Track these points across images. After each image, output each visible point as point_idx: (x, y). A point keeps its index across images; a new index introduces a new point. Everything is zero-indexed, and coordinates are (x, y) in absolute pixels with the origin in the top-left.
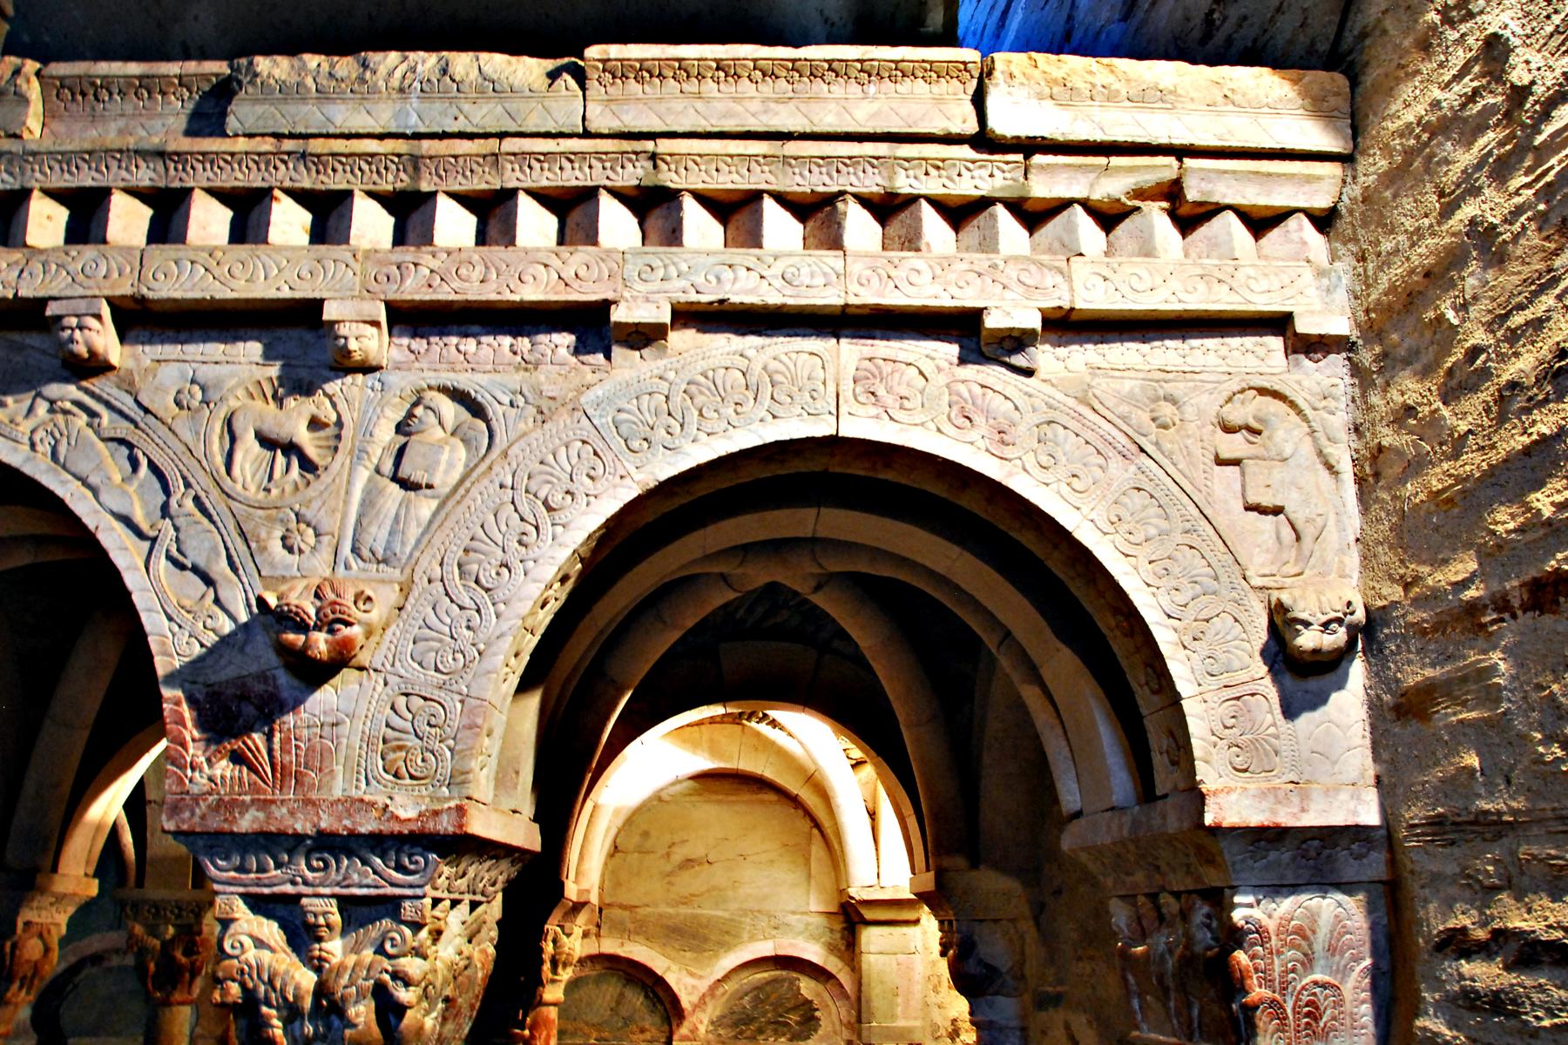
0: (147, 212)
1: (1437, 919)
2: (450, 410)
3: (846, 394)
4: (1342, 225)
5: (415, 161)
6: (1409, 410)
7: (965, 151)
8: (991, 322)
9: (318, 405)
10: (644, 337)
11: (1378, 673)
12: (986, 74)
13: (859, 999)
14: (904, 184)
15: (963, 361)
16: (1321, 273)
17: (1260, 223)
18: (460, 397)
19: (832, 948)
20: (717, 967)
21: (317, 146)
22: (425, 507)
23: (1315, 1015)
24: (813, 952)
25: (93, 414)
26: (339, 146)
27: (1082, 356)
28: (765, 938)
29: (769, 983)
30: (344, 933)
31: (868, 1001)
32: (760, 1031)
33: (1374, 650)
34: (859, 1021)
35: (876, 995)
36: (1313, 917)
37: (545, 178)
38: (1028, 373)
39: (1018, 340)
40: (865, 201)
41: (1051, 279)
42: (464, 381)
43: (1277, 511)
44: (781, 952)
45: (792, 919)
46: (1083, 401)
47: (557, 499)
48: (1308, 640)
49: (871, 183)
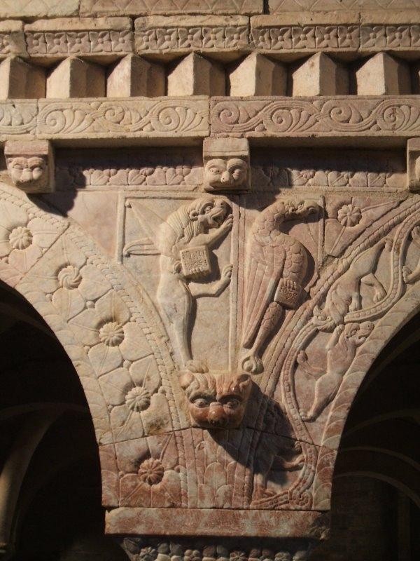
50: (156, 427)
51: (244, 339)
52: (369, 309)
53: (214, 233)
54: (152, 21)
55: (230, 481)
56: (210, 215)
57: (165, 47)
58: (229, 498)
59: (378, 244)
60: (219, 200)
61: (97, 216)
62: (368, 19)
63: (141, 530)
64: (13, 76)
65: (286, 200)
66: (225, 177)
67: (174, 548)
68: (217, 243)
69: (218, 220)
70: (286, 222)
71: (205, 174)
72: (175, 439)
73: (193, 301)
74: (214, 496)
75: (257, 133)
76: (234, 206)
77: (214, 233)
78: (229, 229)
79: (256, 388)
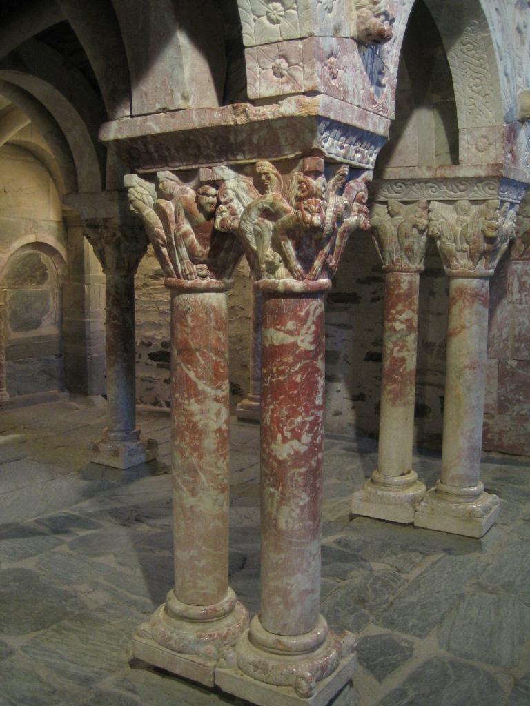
19: (59, 239)
20: (11, 248)
24: (51, 240)
28: (32, 233)
32: (25, 280)
45: (43, 224)
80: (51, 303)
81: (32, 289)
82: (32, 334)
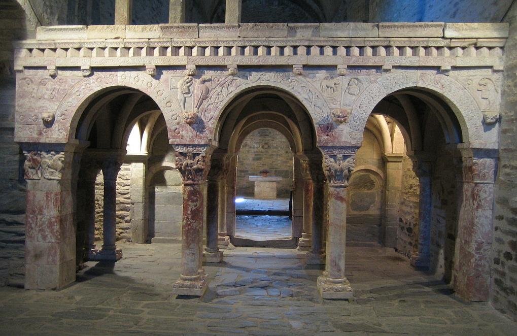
0: (306, 48)
1: (503, 163)
2: (356, 81)
3: (418, 79)
4: (505, 49)
5: (351, 42)
6: (509, 86)
7: (441, 39)
8: (442, 68)
9: (335, 80)
10: (387, 71)
11: (500, 126)
12: (445, 26)
13: (386, 180)
14: (430, 45)
15: (437, 74)
16: (500, 58)
17: (490, 48)
18: (357, 79)
19: (379, 168)
21: (335, 39)
22: (354, 98)
23: (485, 176)
24: (374, 168)
25: (298, 82)
26: (339, 39)
27: (457, 72)
29: (363, 175)
30: (343, 160)
31: (388, 180)
32: (361, 187)
33: (500, 122)
34: (386, 184)
35: (390, 179)
36: (486, 162)
37: (372, 44)
38: (448, 76)
39: (447, 71)
40: (423, 47)
41: (453, 61)
42: (356, 76)
43: (487, 99)
44: (366, 168)
46: (456, 80)
47: (374, 96)
48: (488, 121)
49: (425, 45)
50: (178, 123)
51: (195, 106)
52: (220, 100)
53: (189, 84)
54: (175, 39)
55: (193, 134)
56: (188, 80)
57: (178, 45)
58: (192, 137)
59: (222, 86)
60: (190, 77)
61: (165, 80)
62: (219, 40)
63: (175, 143)
64: (135, 100)
65: (204, 77)
66: (190, 73)
67: (182, 146)
68: (190, 86)
69: (190, 82)
70: (204, 82)
71: (187, 72)
72: (182, 126)
73: (185, 98)
74: (189, 136)
75: (197, 64)
76: (193, 79)
77: (189, 84)
78: (192, 83)
79: (197, 116)
80: (377, 199)
81: (365, 191)
82: (363, 213)
